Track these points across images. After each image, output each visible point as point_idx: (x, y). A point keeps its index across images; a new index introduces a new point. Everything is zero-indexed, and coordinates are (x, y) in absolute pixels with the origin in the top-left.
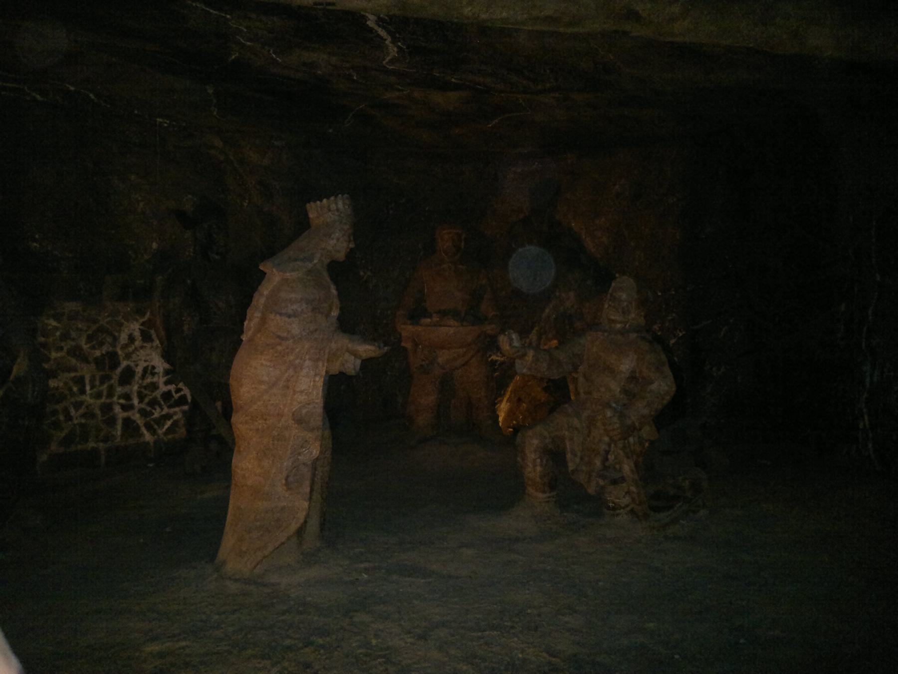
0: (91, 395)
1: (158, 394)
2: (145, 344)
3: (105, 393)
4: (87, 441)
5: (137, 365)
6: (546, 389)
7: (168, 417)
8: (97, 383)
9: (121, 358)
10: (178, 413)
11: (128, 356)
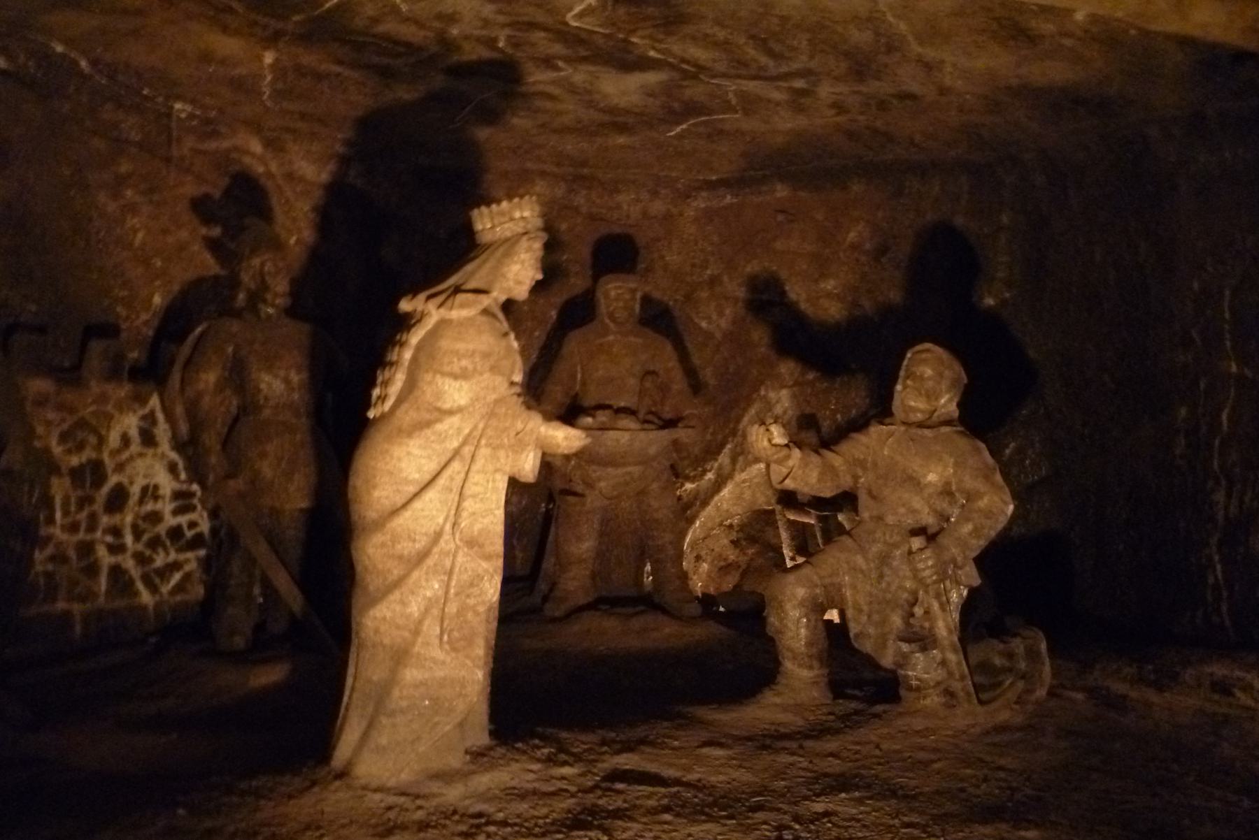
1: (162, 529)
2: (145, 451)
3: (83, 526)
5: (131, 483)
6: (735, 543)
7: (176, 566)
9: (109, 471)
10: (192, 560)
11: (120, 468)
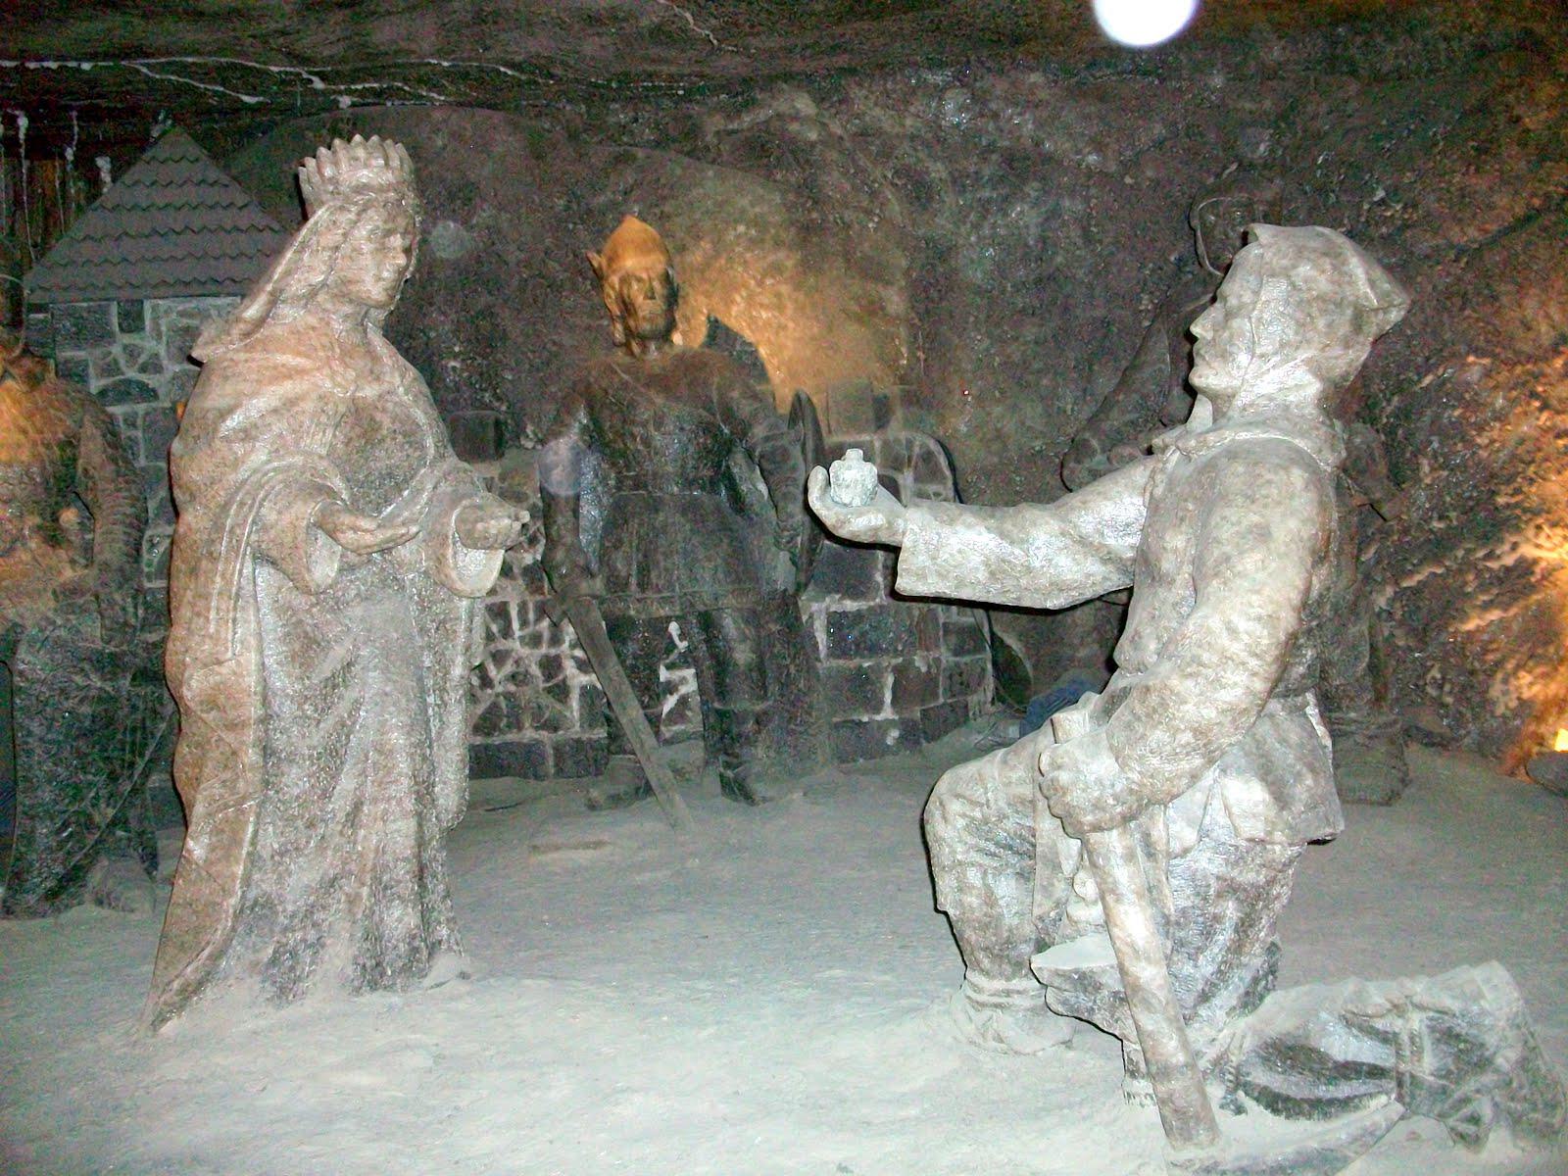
0: (522, 638)
3: (546, 635)
4: (520, 728)
8: (531, 616)
